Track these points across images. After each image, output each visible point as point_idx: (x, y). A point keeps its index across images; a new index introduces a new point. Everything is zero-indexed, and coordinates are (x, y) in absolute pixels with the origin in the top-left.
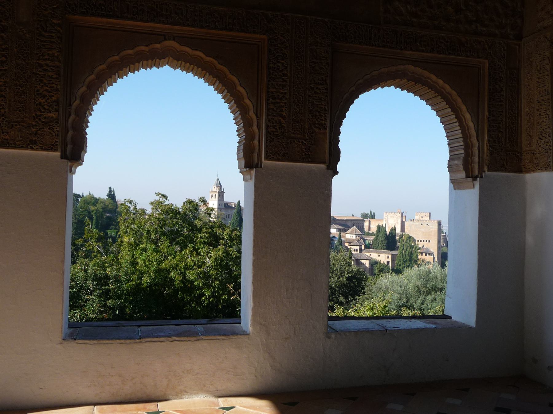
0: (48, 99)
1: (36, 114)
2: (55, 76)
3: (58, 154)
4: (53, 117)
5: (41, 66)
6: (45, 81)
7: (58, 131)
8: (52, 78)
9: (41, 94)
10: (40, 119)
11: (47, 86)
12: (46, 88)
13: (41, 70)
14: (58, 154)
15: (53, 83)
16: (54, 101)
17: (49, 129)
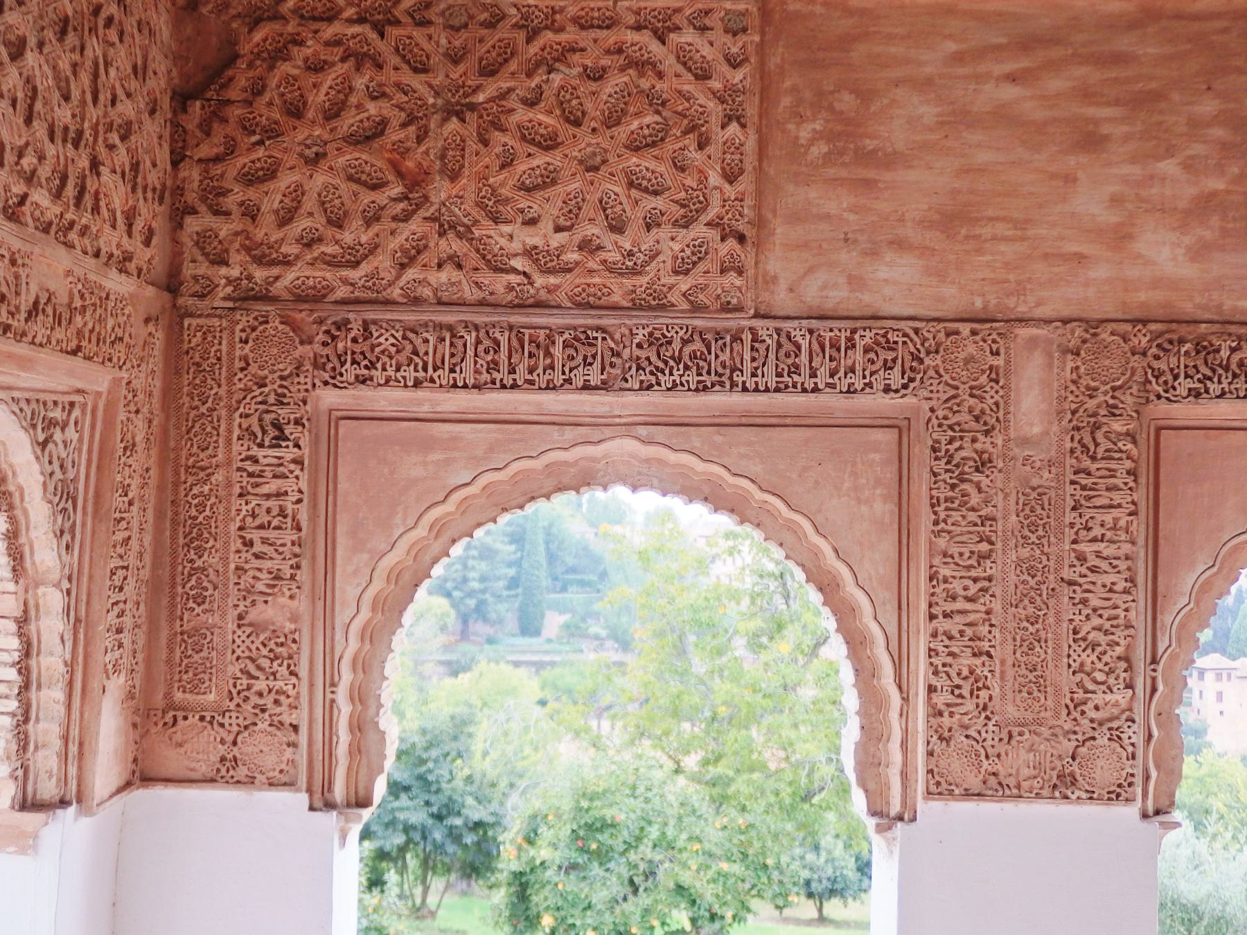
0: (1105, 653)
1: (1072, 700)
2: (1119, 588)
3: (1133, 810)
4: (1116, 704)
5: (1082, 558)
6: (1095, 602)
7: (1133, 745)
8: (1111, 590)
9: (1084, 639)
10: (1083, 713)
11: (1100, 616)
12: (1096, 621)
13: (1084, 570)
14: (1133, 810)
15: (1116, 607)
16: (1119, 658)
17: (1109, 739)
